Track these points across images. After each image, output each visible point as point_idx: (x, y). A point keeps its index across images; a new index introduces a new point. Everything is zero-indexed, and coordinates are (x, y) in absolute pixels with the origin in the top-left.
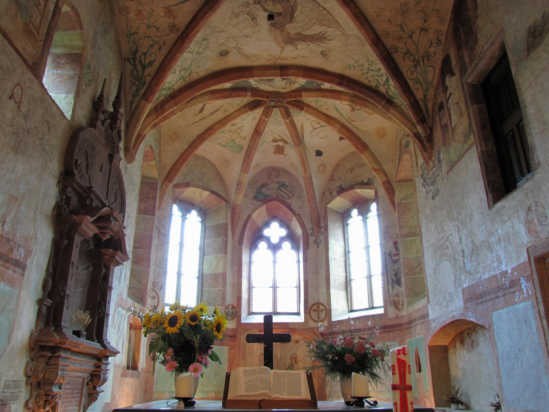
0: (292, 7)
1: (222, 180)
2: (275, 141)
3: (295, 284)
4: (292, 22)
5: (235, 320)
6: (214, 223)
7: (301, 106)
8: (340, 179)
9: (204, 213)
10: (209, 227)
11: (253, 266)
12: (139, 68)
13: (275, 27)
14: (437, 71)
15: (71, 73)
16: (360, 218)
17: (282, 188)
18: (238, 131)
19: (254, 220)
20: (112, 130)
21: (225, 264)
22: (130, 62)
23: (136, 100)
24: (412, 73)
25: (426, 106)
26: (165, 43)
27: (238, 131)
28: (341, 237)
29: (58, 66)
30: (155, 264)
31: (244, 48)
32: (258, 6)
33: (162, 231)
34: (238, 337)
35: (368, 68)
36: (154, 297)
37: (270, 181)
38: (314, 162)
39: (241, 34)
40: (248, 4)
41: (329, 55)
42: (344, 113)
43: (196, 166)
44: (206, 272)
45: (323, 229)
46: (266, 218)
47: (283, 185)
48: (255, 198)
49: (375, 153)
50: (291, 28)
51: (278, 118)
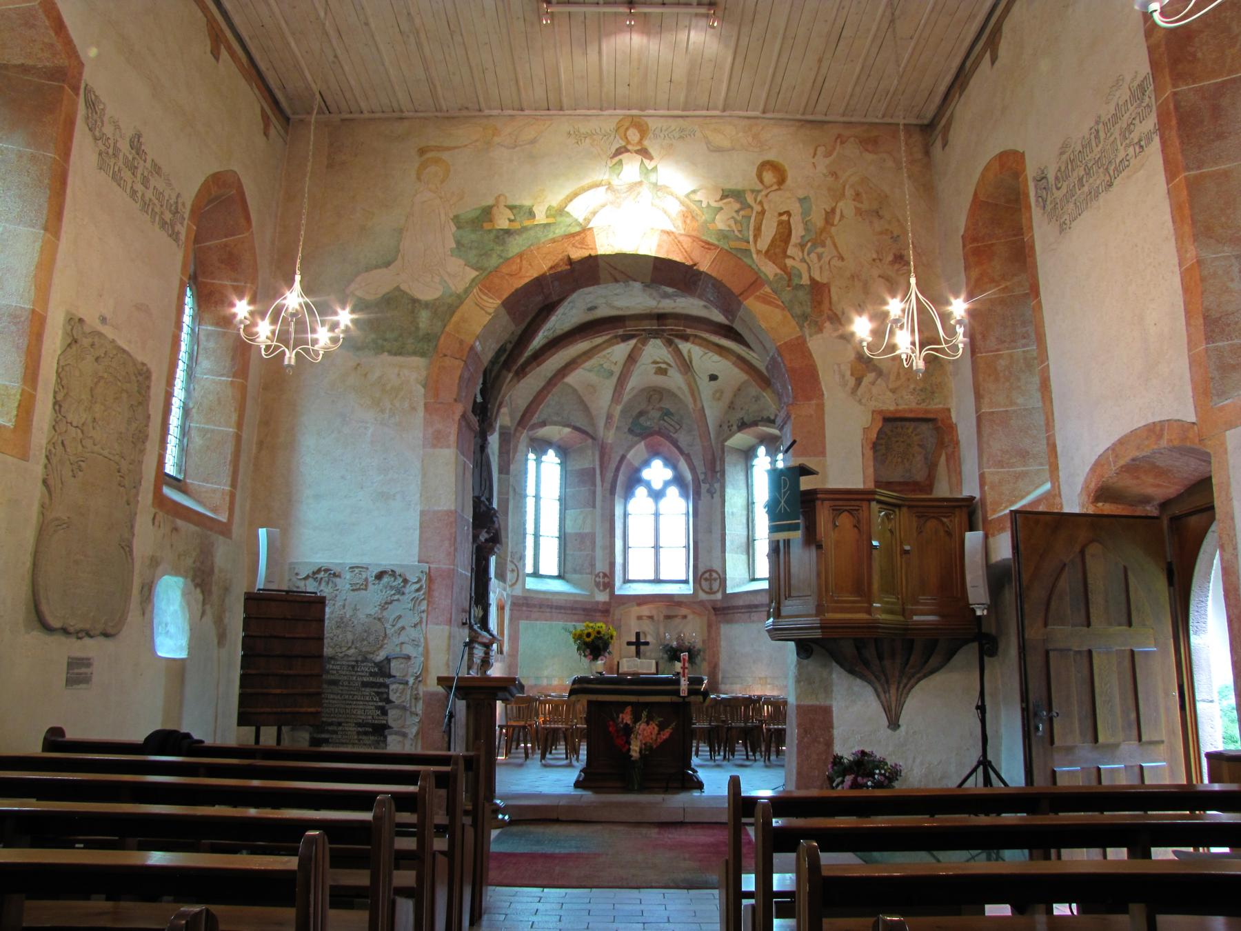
1: (586, 409)
2: (655, 362)
3: (684, 543)
6: (578, 467)
9: (564, 452)
11: (630, 520)
16: (768, 459)
28: (742, 484)
38: (706, 389)
44: (569, 530)
46: (646, 456)
47: (667, 413)
48: (631, 431)
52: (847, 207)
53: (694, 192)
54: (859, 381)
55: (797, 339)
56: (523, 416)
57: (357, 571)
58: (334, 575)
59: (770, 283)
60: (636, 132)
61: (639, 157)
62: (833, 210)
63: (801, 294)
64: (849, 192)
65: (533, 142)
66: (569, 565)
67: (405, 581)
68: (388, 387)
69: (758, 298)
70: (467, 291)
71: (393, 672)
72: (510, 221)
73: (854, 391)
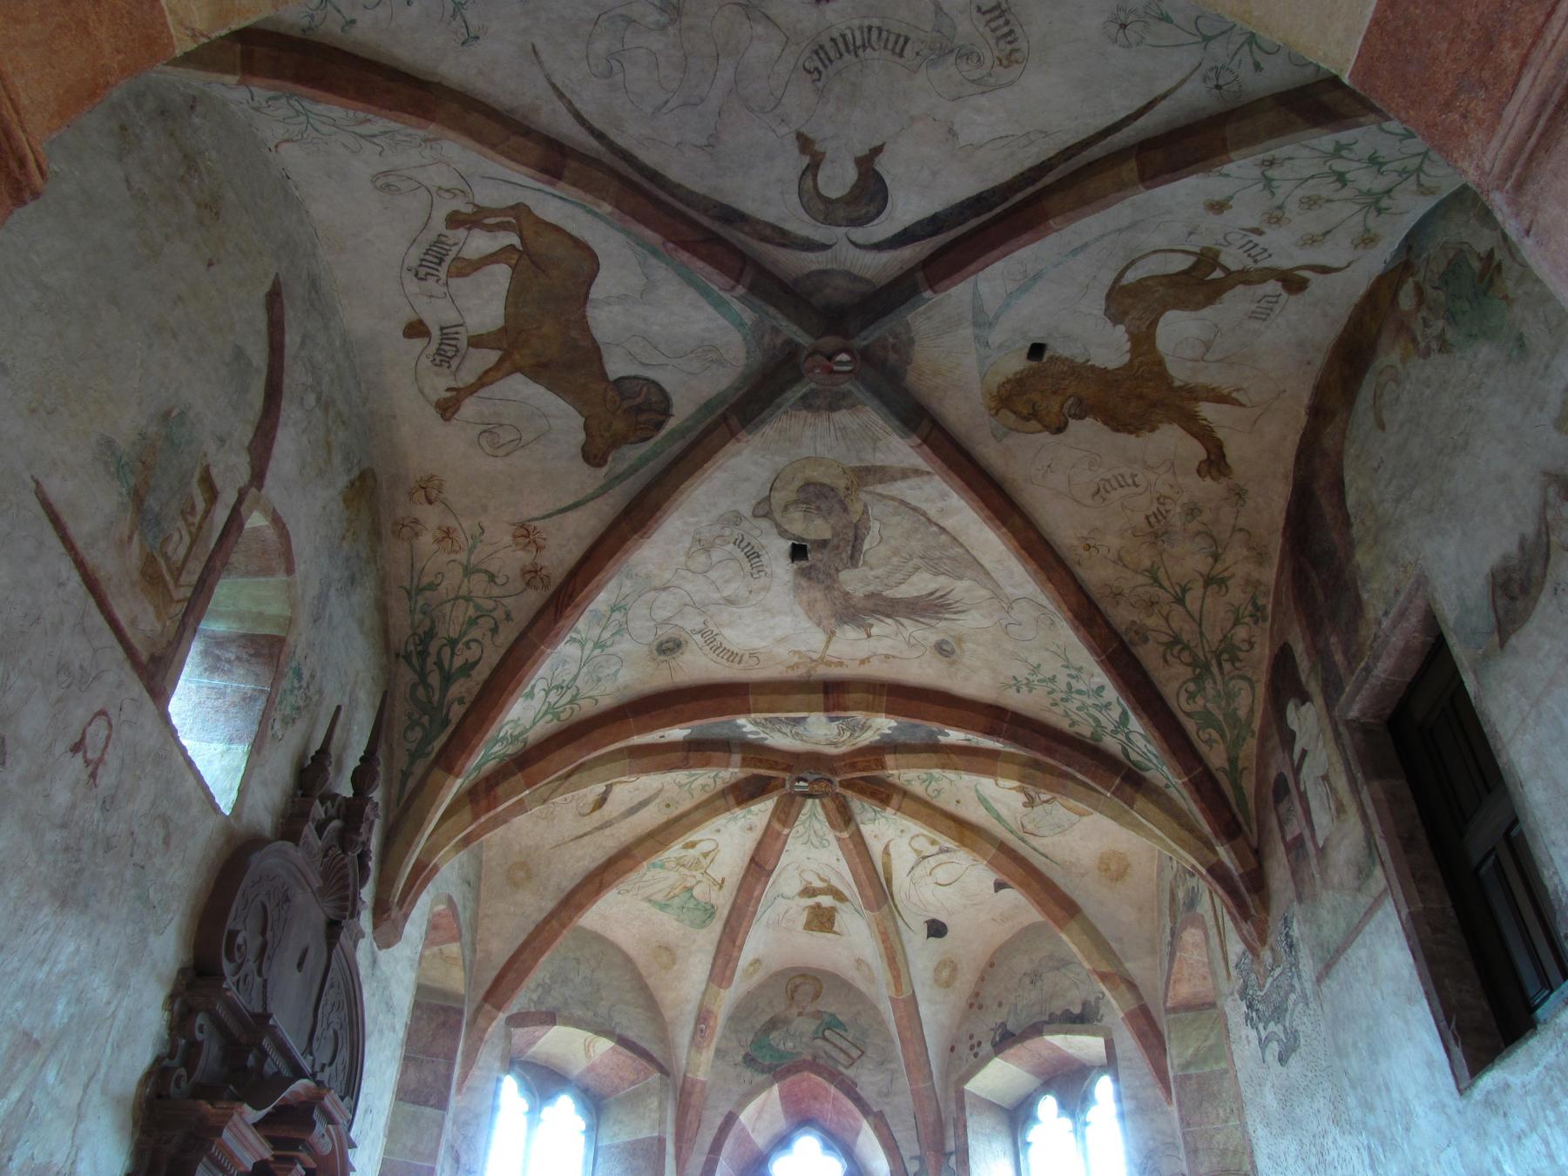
0: (856, 527)
1: (651, 1004)
2: (808, 892)
4: (855, 566)
6: (624, 1137)
7: (883, 794)
8: (1000, 1005)
10: (609, 1147)
12: (434, 679)
13: (810, 579)
14: (1261, 690)
15: (248, 687)
16: (1066, 1122)
17: (827, 1033)
18: (705, 862)
19: (743, 1129)
20: (344, 851)
22: (410, 663)
23: (420, 768)
24: (1191, 696)
25: (1238, 788)
26: (508, 617)
27: (705, 862)
29: (214, 665)
31: (727, 632)
32: (764, 524)
33: (463, 1159)
35: (1069, 685)
37: (795, 1011)
38: (922, 955)
39: (716, 596)
40: (737, 518)
41: (958, 651)
42: (1004, 812)
43: (578, 961)
45: (953, 1159)
47: (832, 1024)
48: (749, 1060)
49: (1099, 926)
50: (854, 582)
51: (817, 826)
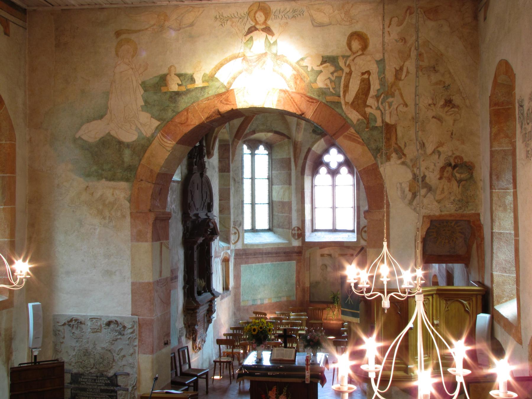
5: (301, 239)
9: (269, 146)
21: (290, 194)
30: (234, 207)
33: (236, 180)
34: (303, 253)
36: (235, 233)
44: (275, 199)
52: (410, 65)
53: (302, 59)
54: (414, 195)
55: (373, 165)
56: (238, 132)
57: (94, 320)
58: (81, 323)
59: (354, 126)
60: (262, 14)
61: (264, 34)
62: (401, 69)
63: (375, 133)
64: (413, 54)
65: (192, 25)
66: (275, 222)
67: (124, 327)
68: (107, 202)
69: (346, 137)
70: (153, 136)
71: (119, 383)
72: (179, 85)
73: (410, 203)
